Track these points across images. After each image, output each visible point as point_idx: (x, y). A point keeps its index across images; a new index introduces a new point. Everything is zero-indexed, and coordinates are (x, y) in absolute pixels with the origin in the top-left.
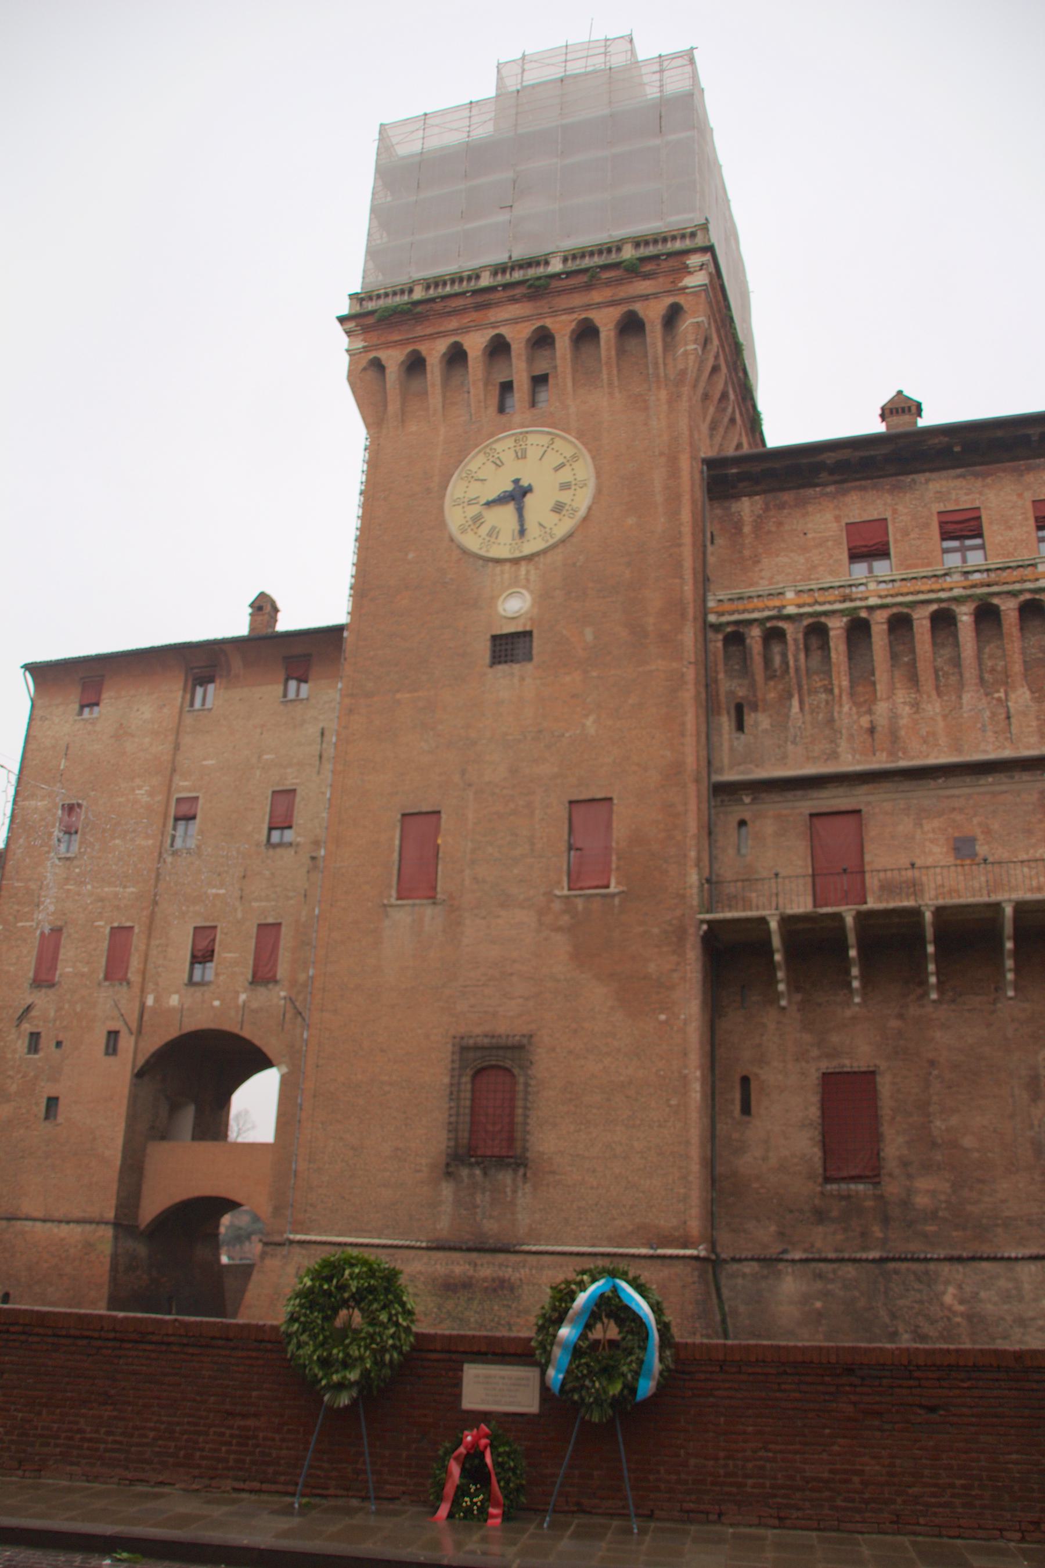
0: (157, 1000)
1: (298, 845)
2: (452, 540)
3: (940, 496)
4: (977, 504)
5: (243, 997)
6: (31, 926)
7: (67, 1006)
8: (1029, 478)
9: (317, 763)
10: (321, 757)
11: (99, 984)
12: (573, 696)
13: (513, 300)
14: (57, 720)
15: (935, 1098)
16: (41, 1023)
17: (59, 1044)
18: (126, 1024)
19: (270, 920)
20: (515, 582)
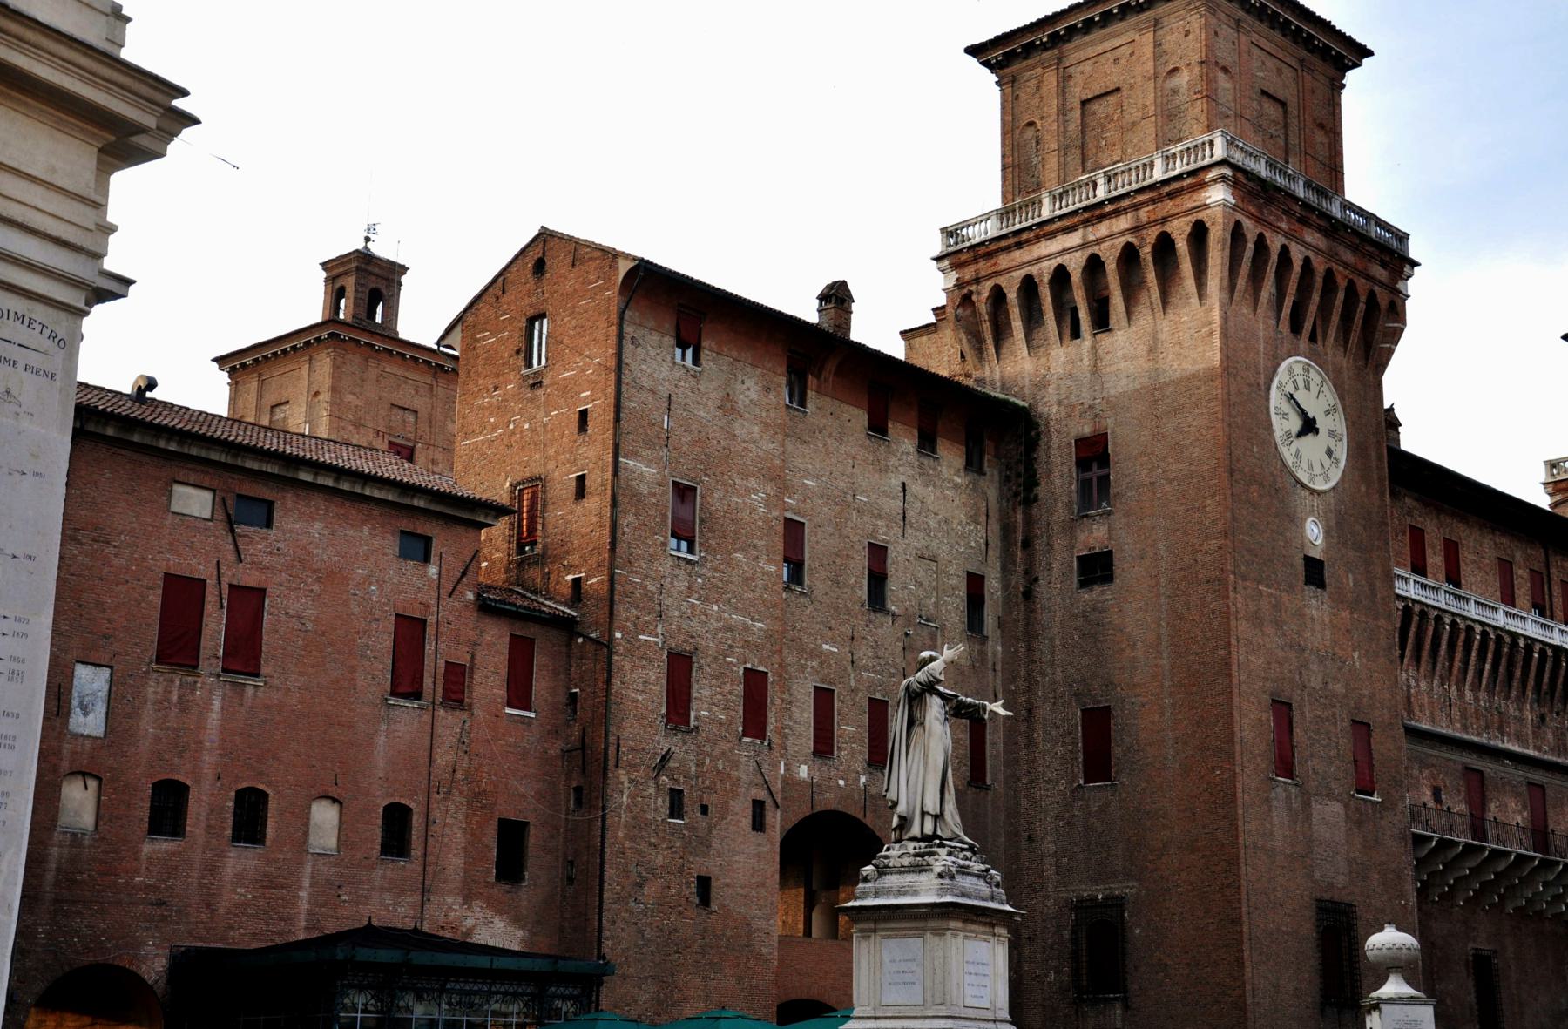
0: (787, 769)
1: (893, 615)
2: (1276, 448)
3: (1410, 513)
4: (1423, 527)
5: (863, 779)
6: (656, 643)
7: (707, 761)
8: (1442, 517)
9: (902, 524)
10: (904, 517)
11: (740, 740)
12: (1348, 631)
13: (1319, 229)
14: (652, 353)
15: (1435, 969)
16: (682, 779)
17: (704, 810)
18: (771, 793)
19: (878, 696)
20: (1312, 512)
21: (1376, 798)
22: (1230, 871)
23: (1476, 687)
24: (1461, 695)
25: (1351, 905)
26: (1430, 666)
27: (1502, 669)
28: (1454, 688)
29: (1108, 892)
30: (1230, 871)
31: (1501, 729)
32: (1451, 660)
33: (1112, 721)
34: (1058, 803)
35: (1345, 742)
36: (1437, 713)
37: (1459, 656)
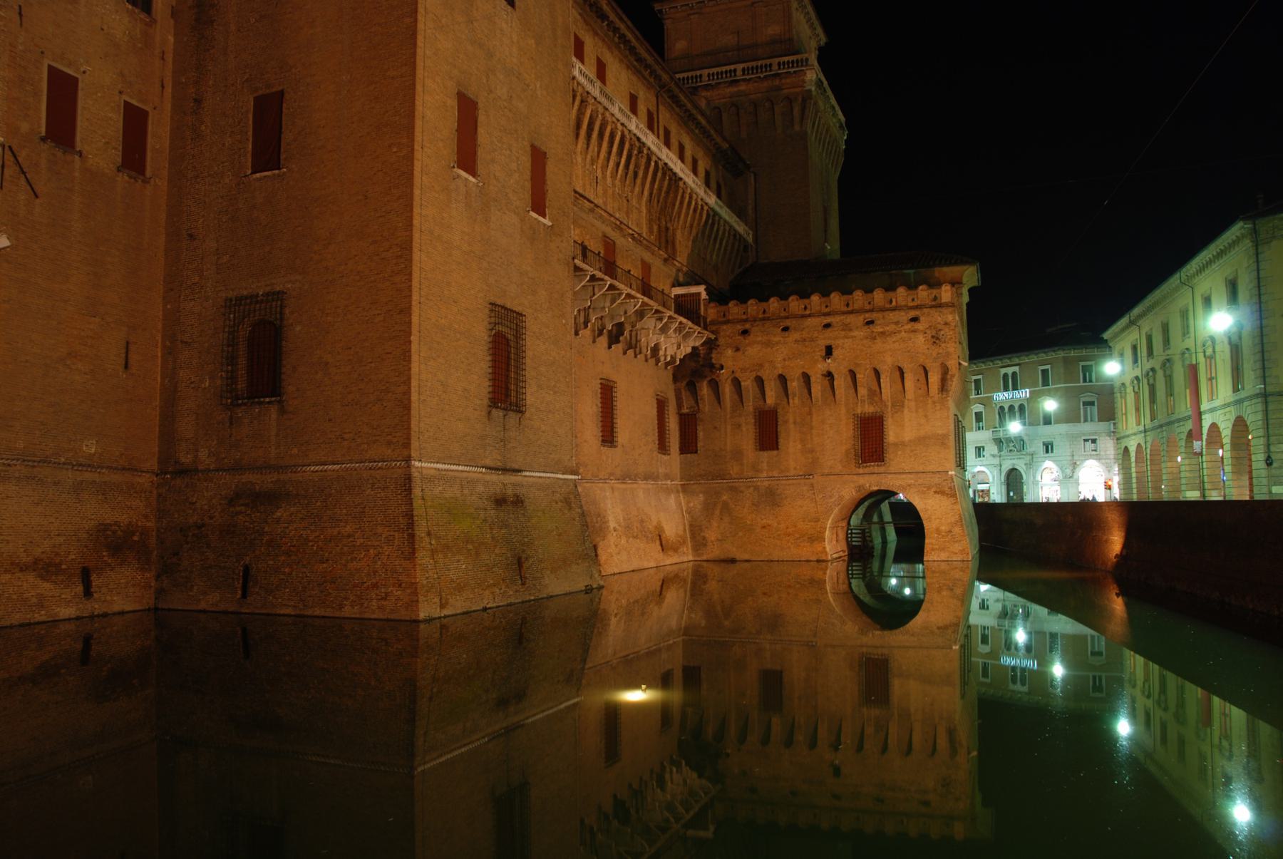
21: (547, 222)
22: (401, 257)
23: (614, 176)
24: (604, 177)
25: (521, 315)
26: (585, 146)
27: (632, 167)
28: (599, 171)
29: (268, 289)
30: (401, 257)
31: (627, 214)
32: (600, 146)
33: (284, 105)
34: (222, 197)
35: (526, 161)
36: (588, 186)
37: (605, 145)
